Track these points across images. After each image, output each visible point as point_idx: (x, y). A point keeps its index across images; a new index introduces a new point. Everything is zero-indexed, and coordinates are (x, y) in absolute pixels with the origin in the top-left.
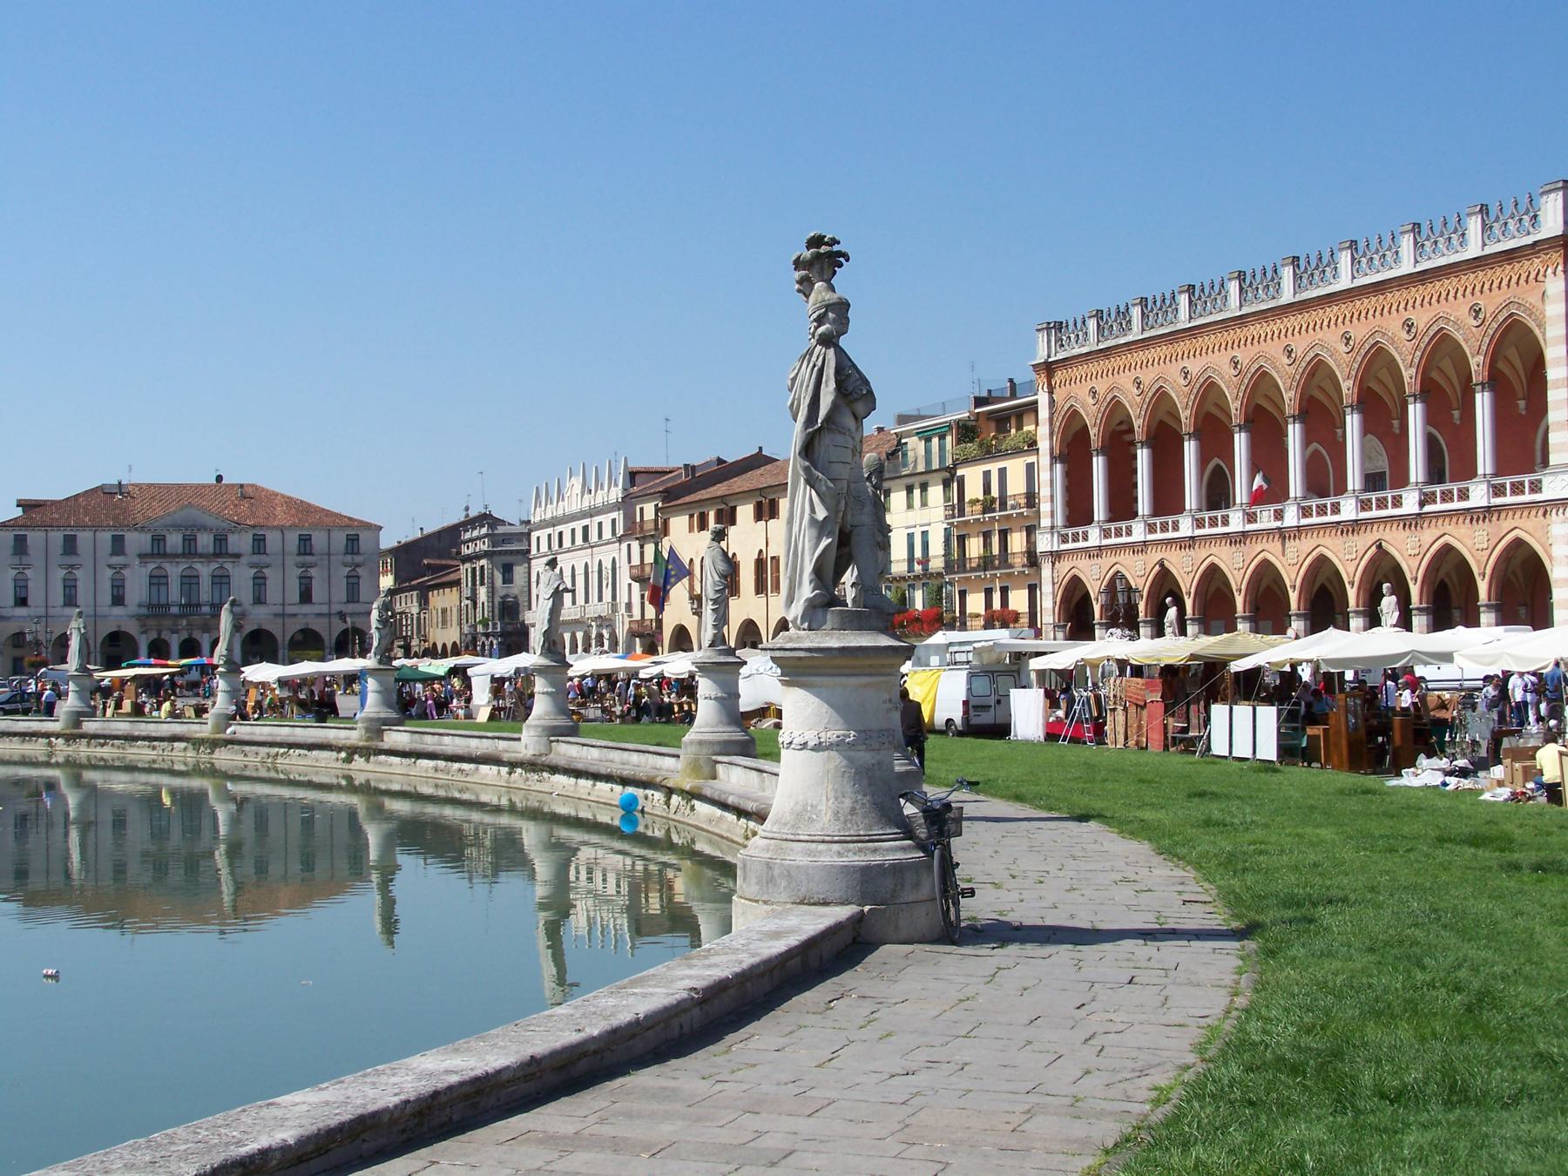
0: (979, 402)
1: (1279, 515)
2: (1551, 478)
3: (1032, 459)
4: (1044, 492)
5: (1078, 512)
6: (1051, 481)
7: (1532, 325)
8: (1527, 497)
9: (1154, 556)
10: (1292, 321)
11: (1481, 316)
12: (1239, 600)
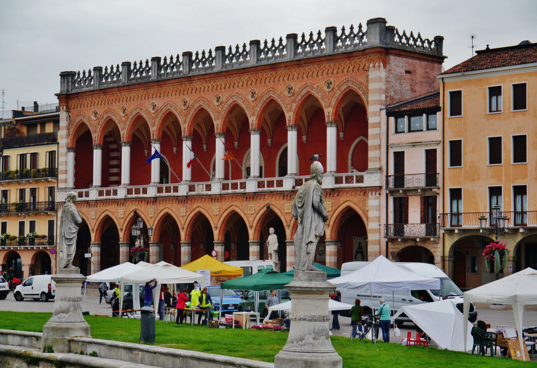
0: (16, 113)
1: (208, 188)
2: (368, 175)
3: (53, 148)
4: (61, 168)
5: (83, 179)
6: (67, 162)
7: (360, 92)
8: (355, 185)
9: (132, 207)
10: (221, 82)
11: (332, 86)
12: (183, 234)
